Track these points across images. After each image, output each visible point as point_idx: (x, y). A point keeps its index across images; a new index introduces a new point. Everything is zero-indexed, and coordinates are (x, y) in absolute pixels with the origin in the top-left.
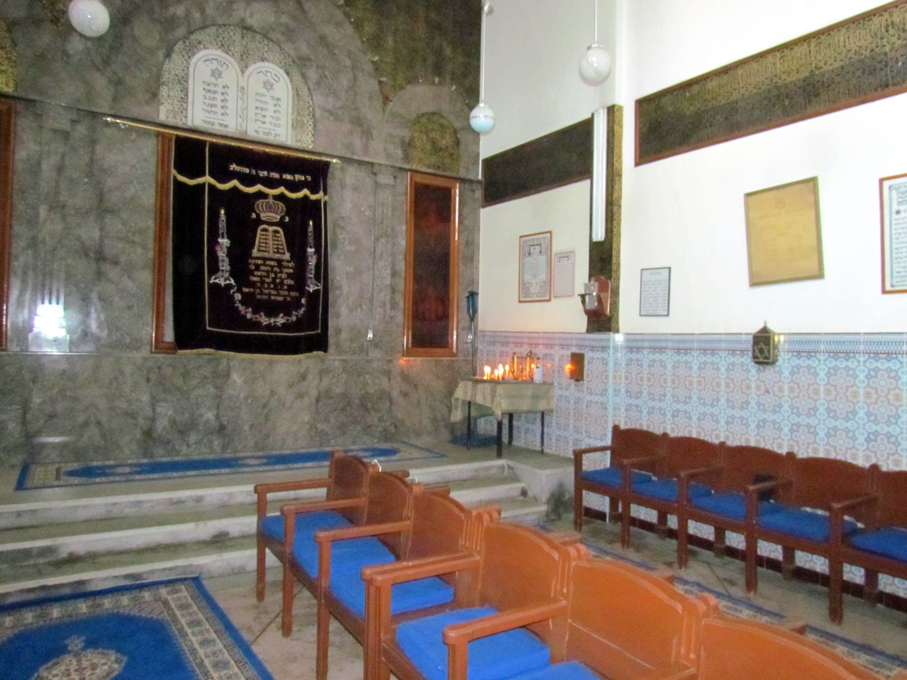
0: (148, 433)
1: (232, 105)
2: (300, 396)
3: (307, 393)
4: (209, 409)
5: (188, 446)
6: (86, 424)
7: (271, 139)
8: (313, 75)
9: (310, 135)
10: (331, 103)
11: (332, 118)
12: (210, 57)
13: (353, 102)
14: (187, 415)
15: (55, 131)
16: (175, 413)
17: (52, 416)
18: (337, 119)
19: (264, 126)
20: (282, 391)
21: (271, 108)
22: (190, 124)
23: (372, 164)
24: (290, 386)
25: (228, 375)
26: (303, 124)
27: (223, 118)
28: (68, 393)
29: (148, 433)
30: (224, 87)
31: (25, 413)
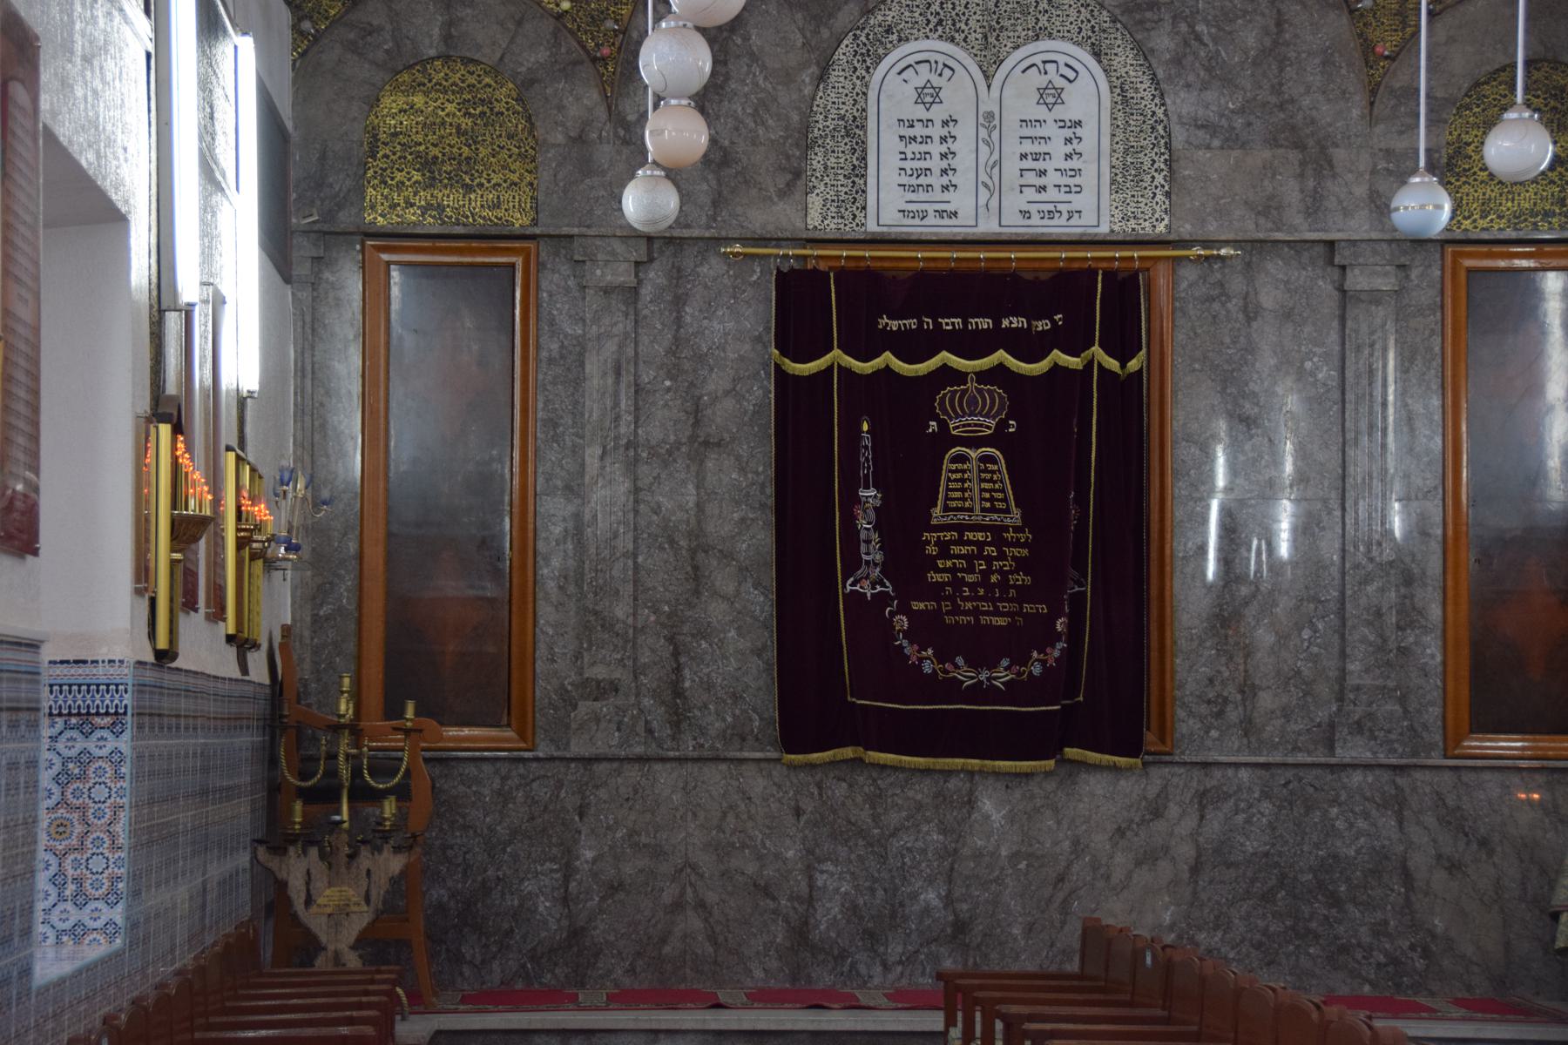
0: (800, 932)
1: (964, 160)
2: (1148, 858)
3: (1166, 849)
4: (930, 881)
5: (886, 967)
6: (678, 906)
7: (1057, 227)
8: (1163, 42)
9: (1159, 197)
10: (1217, 102)
11: (1216, 143)
12: (911, 60)
13: (1277, 89)
14: (880, 893)
15: (607, 291)
16: (856, 887)
17: (614, 888)
18: (1232, 141)
19: (1043, 196)
20: (1100, 841)
21: (1058, 148)
22: (872, 227)
23: (1331, 244)
24: (1121, 832)
25: (970, 803)
26: (1140, 171)
27: (946, 196)
28: (644, 839)
29: (800, 932)
30: (945, 123)
31: (567, 879)
